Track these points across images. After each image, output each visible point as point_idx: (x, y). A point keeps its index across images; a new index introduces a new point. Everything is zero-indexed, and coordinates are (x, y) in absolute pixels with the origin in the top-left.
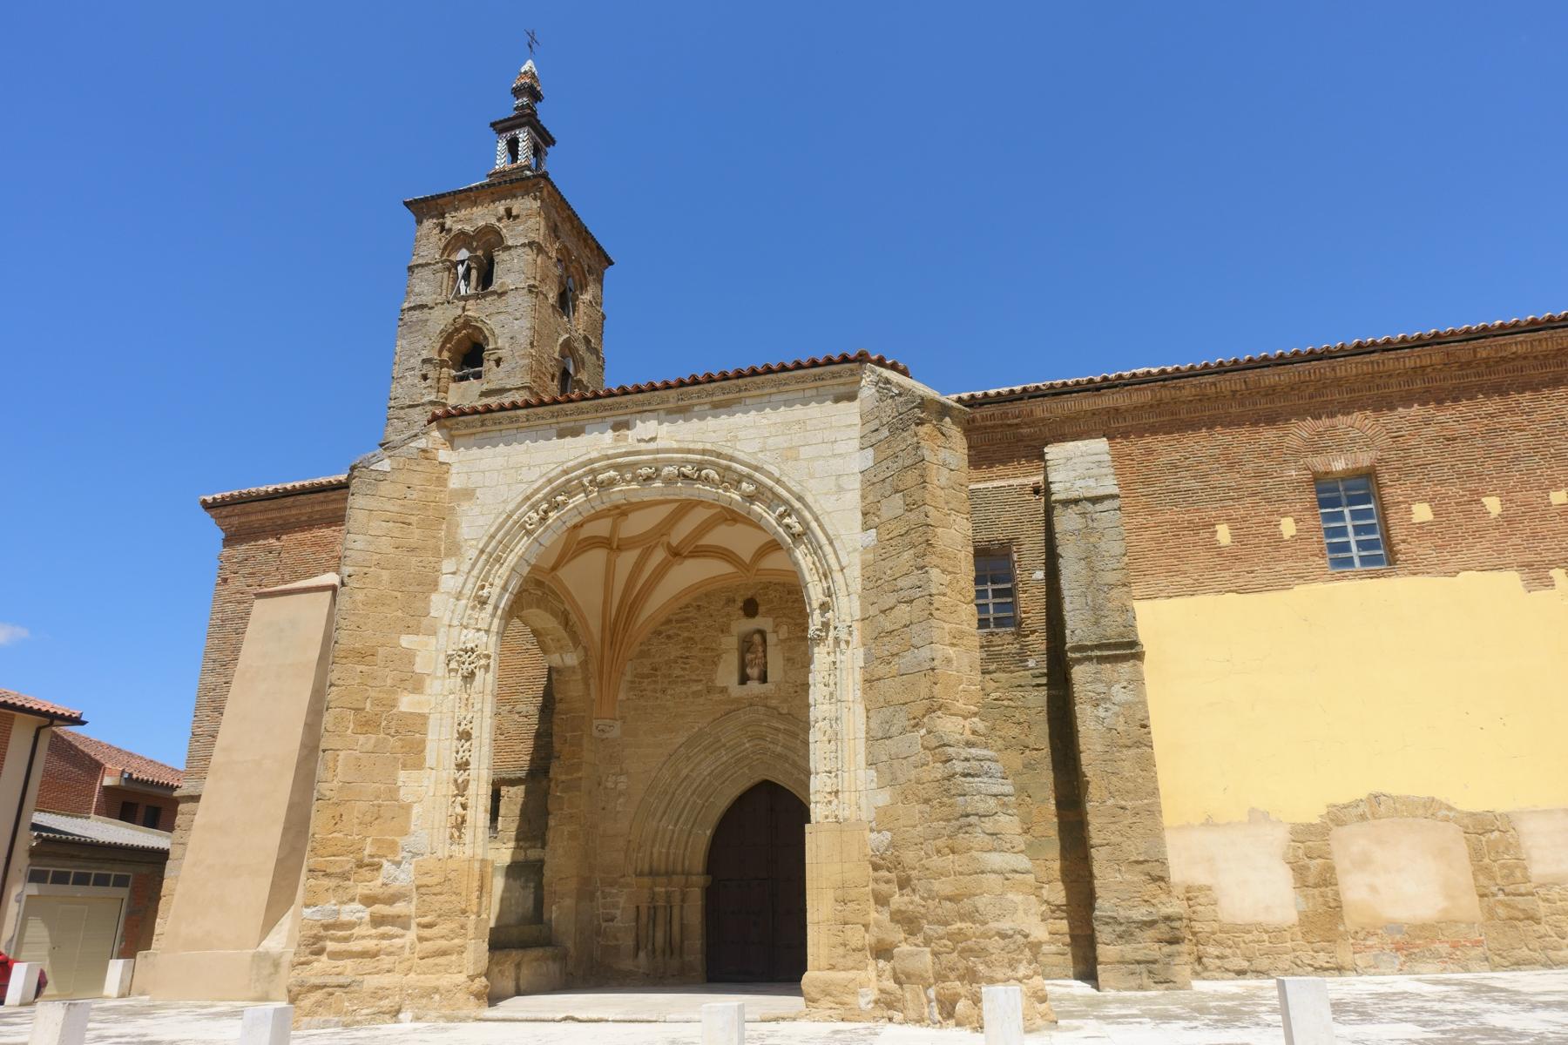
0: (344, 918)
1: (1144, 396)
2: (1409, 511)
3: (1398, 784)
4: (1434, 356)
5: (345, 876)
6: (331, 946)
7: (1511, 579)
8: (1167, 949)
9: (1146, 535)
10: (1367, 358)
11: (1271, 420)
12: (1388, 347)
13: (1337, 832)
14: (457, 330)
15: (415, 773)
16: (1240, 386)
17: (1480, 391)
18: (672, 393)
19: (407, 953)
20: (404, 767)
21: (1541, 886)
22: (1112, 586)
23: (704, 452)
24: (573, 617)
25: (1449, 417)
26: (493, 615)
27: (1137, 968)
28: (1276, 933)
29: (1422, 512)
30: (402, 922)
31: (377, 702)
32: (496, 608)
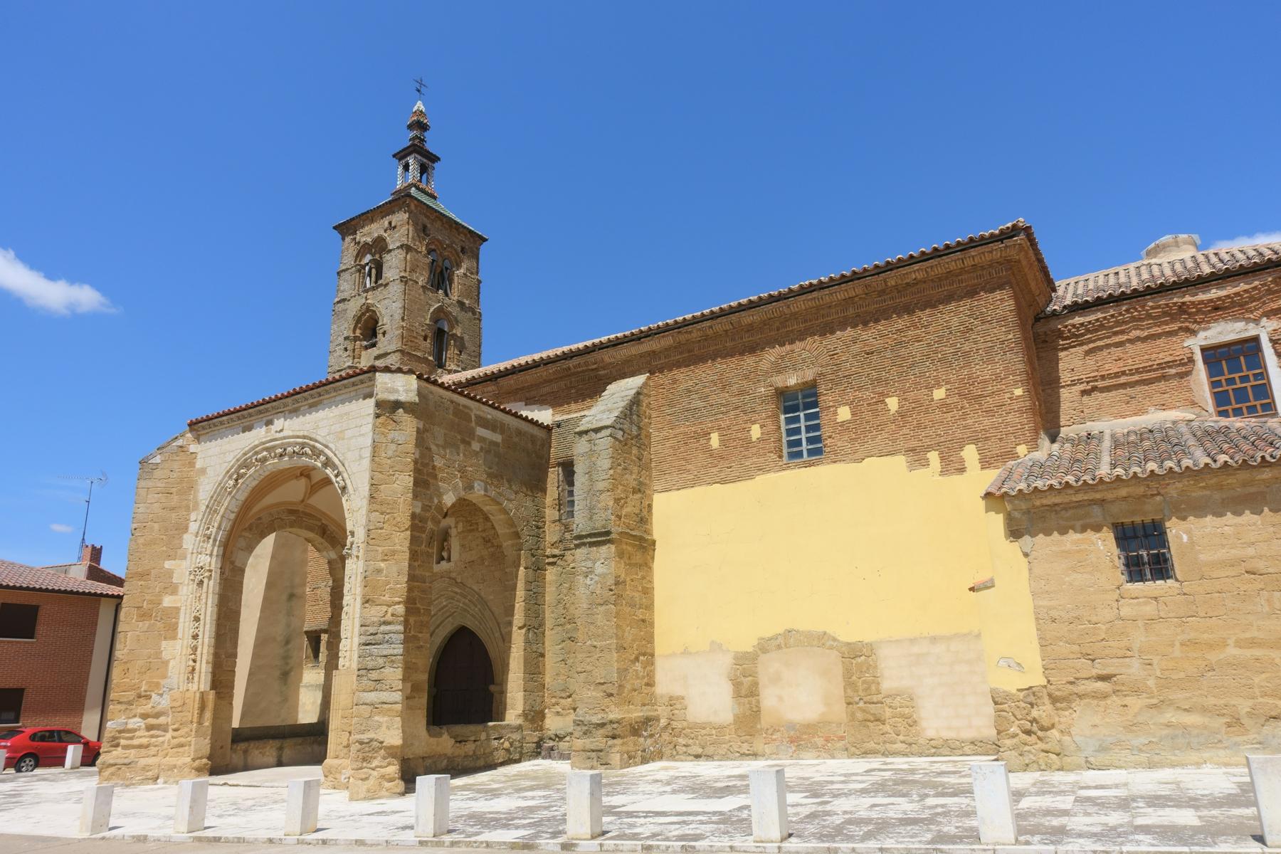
0: (130, 726)
1: (667, 341)
2: (835, 413)
3: (805, 624)
4: (855, 289)
5: (130, 703)
6: (123, 742)
7: (900, 461)
8: (611, 742)
9: (668, 444)
10: (810, 296)
11: (752, 349)
12: (821, 286)
13: (763, 658)
14: (363, 314)
15: (171, 642)
16: (729, 327)
17: (894, 312)
18: (289, 400)
19: (166, 745)
20: (165, 639)
21: (887, 697)
22: (601, 492)
23: (304, 437)
24: (332, 527)
25: (870, 335)
26: (214, 545)
27: (594, 754)
28: (720, 728)
29: (844, 413)
30: (164, 728)
31: (151, 602)
32: (215, 540)
